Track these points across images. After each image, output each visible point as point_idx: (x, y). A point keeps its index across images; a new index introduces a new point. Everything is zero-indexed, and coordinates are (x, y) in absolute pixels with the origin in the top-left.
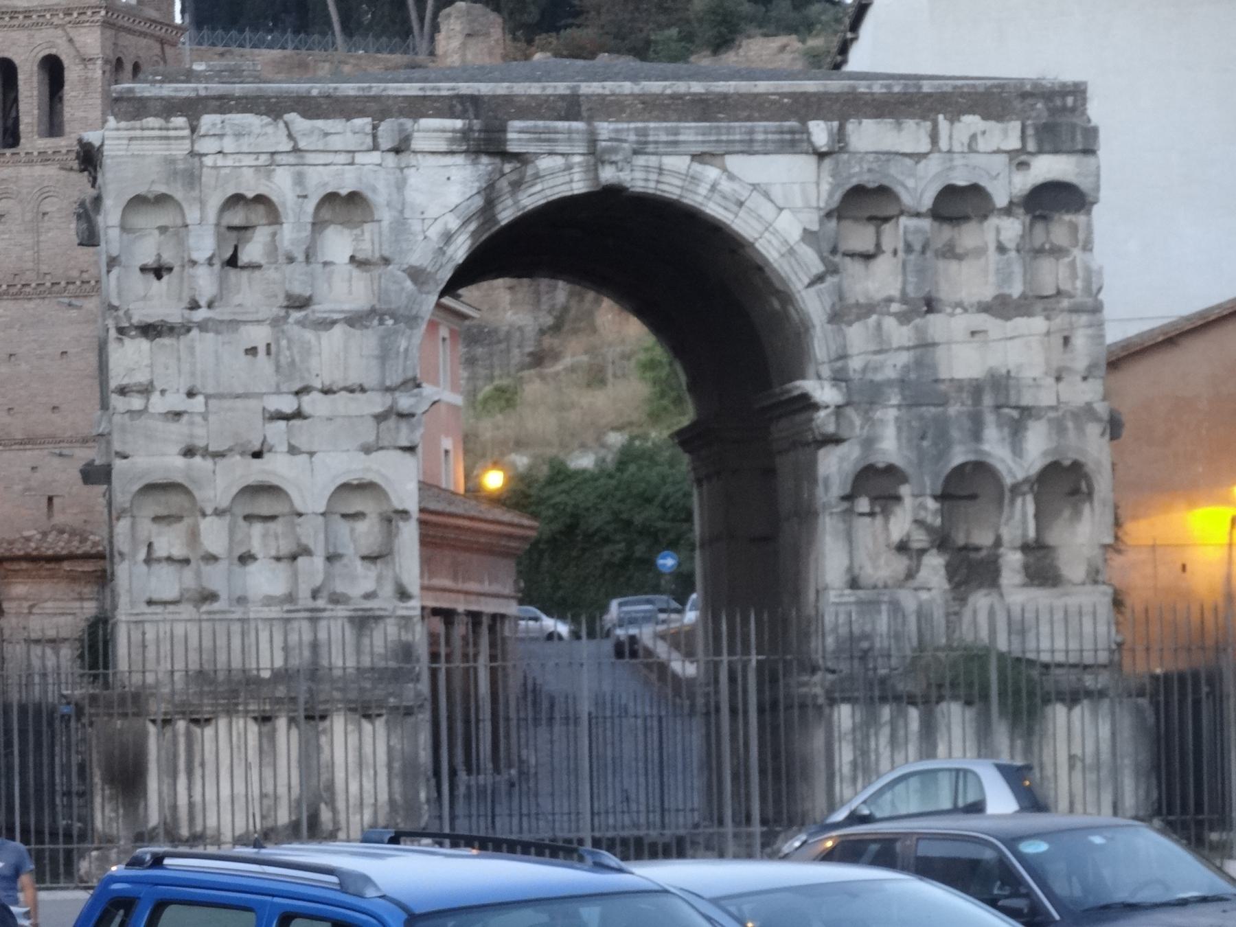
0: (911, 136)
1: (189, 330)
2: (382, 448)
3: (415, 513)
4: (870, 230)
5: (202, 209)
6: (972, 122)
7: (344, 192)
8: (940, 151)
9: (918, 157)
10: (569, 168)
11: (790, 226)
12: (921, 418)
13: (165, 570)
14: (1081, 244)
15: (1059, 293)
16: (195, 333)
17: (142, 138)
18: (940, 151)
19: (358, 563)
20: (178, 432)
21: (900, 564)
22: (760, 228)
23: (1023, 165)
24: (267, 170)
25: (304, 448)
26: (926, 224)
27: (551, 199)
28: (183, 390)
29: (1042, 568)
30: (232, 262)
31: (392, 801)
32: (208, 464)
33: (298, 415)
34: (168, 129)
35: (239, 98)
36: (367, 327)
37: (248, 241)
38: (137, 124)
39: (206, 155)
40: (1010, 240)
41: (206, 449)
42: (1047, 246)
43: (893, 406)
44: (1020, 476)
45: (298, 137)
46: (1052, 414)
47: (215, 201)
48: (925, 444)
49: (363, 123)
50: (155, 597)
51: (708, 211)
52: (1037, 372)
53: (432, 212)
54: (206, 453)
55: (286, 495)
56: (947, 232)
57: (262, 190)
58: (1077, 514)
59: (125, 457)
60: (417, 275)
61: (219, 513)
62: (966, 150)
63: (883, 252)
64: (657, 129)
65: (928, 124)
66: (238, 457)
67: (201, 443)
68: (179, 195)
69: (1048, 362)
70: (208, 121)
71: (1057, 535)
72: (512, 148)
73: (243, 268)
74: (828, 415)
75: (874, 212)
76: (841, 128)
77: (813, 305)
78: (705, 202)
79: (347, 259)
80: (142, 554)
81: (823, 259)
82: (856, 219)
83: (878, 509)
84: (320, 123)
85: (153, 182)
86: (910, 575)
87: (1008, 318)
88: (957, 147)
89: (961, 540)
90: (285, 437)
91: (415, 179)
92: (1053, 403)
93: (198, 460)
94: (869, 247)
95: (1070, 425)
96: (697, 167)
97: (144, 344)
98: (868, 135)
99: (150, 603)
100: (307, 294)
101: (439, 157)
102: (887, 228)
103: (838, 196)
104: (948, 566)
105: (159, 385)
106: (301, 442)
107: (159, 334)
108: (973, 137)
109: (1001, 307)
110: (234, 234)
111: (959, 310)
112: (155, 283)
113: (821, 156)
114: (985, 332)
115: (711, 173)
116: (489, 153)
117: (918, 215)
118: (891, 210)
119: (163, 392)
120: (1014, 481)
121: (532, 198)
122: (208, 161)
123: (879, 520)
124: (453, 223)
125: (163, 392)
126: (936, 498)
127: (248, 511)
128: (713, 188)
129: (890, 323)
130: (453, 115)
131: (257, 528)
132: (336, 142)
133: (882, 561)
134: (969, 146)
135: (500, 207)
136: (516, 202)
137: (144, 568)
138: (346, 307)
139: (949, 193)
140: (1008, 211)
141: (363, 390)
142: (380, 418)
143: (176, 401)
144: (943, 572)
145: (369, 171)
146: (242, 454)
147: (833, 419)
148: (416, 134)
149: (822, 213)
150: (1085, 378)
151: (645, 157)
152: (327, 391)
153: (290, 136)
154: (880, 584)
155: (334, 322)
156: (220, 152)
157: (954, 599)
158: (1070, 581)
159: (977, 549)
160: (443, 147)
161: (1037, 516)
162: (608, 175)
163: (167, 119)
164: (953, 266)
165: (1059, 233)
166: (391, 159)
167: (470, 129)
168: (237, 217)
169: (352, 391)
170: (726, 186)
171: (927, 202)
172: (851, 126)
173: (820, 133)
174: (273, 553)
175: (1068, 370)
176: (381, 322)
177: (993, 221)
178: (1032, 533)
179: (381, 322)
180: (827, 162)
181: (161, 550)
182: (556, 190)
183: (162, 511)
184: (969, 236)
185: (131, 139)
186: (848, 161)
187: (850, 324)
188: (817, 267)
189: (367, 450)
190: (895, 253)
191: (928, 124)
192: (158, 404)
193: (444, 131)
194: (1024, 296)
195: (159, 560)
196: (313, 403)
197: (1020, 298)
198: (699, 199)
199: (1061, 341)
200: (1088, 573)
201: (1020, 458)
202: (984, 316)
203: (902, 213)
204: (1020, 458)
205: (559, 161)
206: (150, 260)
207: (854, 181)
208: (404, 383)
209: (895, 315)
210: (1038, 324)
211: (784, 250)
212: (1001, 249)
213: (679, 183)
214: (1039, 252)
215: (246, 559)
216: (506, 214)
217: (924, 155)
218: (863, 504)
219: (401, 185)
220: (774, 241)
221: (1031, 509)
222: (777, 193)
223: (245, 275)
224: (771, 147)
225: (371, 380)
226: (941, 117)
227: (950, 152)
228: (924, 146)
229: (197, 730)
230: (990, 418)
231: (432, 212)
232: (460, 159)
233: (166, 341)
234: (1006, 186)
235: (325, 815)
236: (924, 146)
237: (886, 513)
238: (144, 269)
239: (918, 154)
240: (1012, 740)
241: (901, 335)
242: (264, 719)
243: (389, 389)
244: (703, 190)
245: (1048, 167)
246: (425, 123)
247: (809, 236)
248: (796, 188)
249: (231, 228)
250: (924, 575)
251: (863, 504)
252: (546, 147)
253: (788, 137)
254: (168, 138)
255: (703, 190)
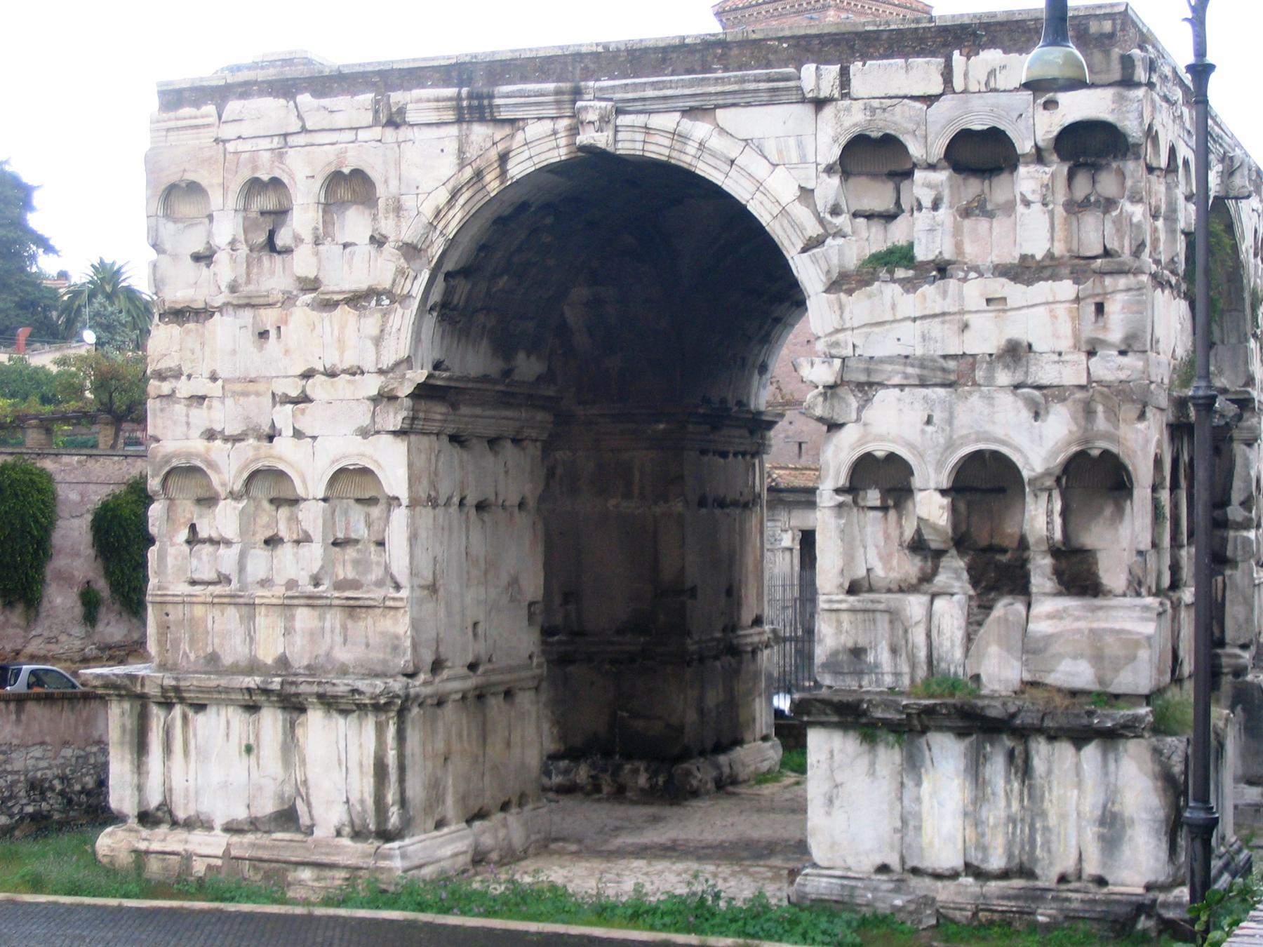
0: (922, 74)
1: (212, 316)
2: (378, 432)
3: (405, 501)
4: (890, 186)
5: (225, 195)
6: (991, 57)
7: (346, 171)
8: (954, 92)
9: (929, 100)
10: (555, 133)
11: (783, 186)
12: (925, 398)
13: (207, 549)
14: (1127, 193)
15: (1107, 253)
16: (217, 315)
17: (178, 129)
18: (954, 92)
19: (373, 548)
20: (201, 418)
21: (911, 567)
22: (752, 188)
23: (1050, 105)
24: (279, 154)
25: (309, 433)
26: (942, 176)
27: (538, 166)
28: (206, 374)
29: (1078, 576)
30: (270, 245)
31: (362, 802)
32: (229, 445)
33: (304, 399)
34: (196, 118)
35: (263, 82)
36: (365, 308)
37: (283, 223)
38: (172, 115)
39: (229, 141)
40: (1033, 192)
41: (222, 432)
42: (1092, 199)
43: (895, 386)
44: (1039, 468)
45: (305, 116)
46: (1079, 395)
47: (236, 184)
48: (930, 429)
49: (367, 98)
50: (196, 576)
51: (698, 172)
52: (1065, 344)
53: (425, 187)
54: (226, 439)
55: (290, 477)
56: (974, 186)
57: (277, 173)
58: (1120, 511)
59: (158, 440)
60: (411, 251)
61: (233, 496)
62: (983, 89)
63: (903, 211)
64: (645, 85)
65: (942, 60)
66: (251, 441)
67: (218, 428)
68: (204, 183)
69: (1076, 334)
70: (234, 107)
71: (1094, 537)
72: (504, 115)
73: (279, 253)
74: (815, 397)
75: (893, 167)
76: (844, 75)
77: (808, 272)
78: (694, 162)
79: (367, 240)
80: (184, 534)
81: (821, 221)
82: (874, 176)
83: (891, 503)
84: (326, 102)
85: (185, 171)
86: (926, 578)
87: (1029, 283)
88: (973, 87)
89: (984, 541)
90: (290, 421)
91: (409, 151)
92: (1084, 381)
93: (218, 443)
94: (886, 204)
95: (1100, 408)
96: (687, 125)
97: (175, 330)
98: (877, 78)
99: (193, 583)
100: (312, 276)
101: (434, 129)
102: (904, 186)
103: (836, 152)
104: (970, 569)
105: (186, 371)
106: (305, 425)
107: (188, 321)
108: (992, 73)
109: (1025, 271)
110: (269, 219)
111: (972, 275)
112: (205, 268)
113: (819, 104)
114: (1004, 299)
115: (699, 129)
116: (482, 120)
117: (932, 167)
118: (909, 166)
119: (189, 377)
120: (1033, 474)
121: (518, 168)
122: (230, 147)
123: (892, 514)
124: (442, 196)
125: (189, 377)
126: (943, 492)
127: (273, 494)
128: (701, 146)
129: (897, 288)
130: (447, 83)
131: (284, 512)
132: (340, 120)
133: (895, 562)
134: (987, 84)
135: (488, 178)
136: (503, 173)
137: (186, 548)
138: (346, 287)
139: (964, 138)
140: (1039, 156)
141: (363, 373)
142: (376, 400)
143: (200, 386)
144: (965, 576)
145: (367, 151)
146: (259, 438)
147: (821, 399)
148: (409, 106)
149: (821, 168)
150: (1123, 353)
151: (632, 117)
152: (331, 374)
153: (299, 116)
154: (894, 586)
155: (336, 304)
156: (239, 137)
157: (979, 607)
158: (1110, 592)
159: (1003, 551)
160: (433, 117)
161: (1064, 514)
162: (588, 137)
163: (198, 107)
164: (983, 224)
165: (1107, 184)
166: (390, 131)
167: (459, 98)
168: (269, 201)
169: (354, 374)
170: (716, 142)
171: (938, 149)
172: (856, 67)
173: (816, 77)
174: (295, 537)
175: (1104, 343)
176: (378, 303)
177: (1022, 170)
178: (1058, 535)
179: (378, 303)
180: (828, 111)
181: (203, 533)
182: (543, 157)
183: (202, 493)
184: (999, 190)
185: (168, 130)
186: (848, 109)
187: (850, 292)
188: (814, 229)
189: (364, 433)
190: (912, 210)
191: (942, 60)
192: (184, 388)
193: (437, 100)
194: (1050, 255)
195: (203, 541)
196: (317, 387)
197: (1045, 257)
198: (688, 159)
199: (1093, 308)
200: (1130, 583)
201: (1038, 445)
202: (1003, 280)
203: (915, 165)
204: (1038, 445)
205: (547, 126)
206: (200, 248)
207: (856, 131)
208: (397, 364)
209: (901, 281)
210: (1066, 288)
211: (776, 211)
212: (1027, 203)
213: (667, 142)
214: (1085, 205)
215: (272, 542)
216: (493, 185)
217: (936, 98)
218: (873, 497)
219: (398, 163)
220: (766, 201)
221: (1058, 506)
222: (770, 148)
223: (278, 258)
224: (765, 97)
225: (369, 365)
226: (956, 53)
227: (965, 91)
228: (936, 87)
229: (191, 714)
230: (1006, 400)
231: (425, 187)
232: (453, 130)
233: (191, 326)
234: (1035, 127)
235: (301, 807)
236: (936, 87)
237: (898, 506)
238: (197, 258)
239: (930, 97)
240: (1008, 781)
241: (909, 303)
242: (252, 708)
243: (381, 372)
244: (691, 149)
245: (1079, 106)
246: (418, 93)
247: (806, 194)
248: (792, 142)
249: (262, 213)
250: (942, 579)
251: (873, 497)
252: (533, 112)
253: (781, 84)
254: (197, 127)
255: (691, 149)
